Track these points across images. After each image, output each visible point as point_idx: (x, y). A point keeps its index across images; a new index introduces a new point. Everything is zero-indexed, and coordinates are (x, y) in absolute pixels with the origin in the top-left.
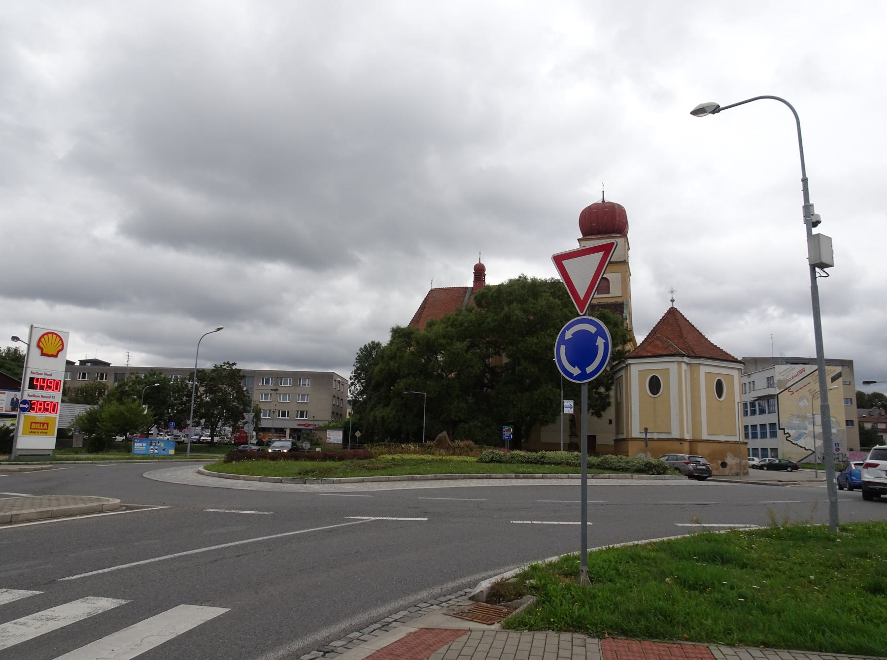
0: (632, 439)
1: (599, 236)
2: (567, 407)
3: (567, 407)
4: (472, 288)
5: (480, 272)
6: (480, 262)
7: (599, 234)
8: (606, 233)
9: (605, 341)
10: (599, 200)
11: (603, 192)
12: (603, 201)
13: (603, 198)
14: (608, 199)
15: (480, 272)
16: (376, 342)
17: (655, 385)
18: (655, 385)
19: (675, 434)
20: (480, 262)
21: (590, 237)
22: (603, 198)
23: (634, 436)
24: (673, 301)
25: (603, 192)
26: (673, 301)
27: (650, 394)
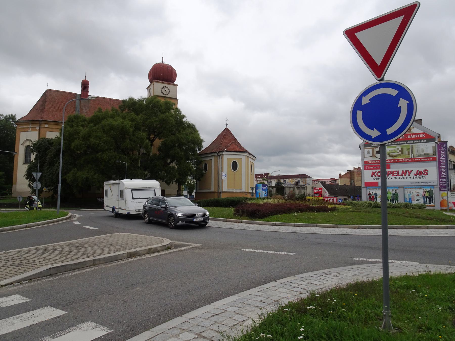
0: (223, 192)
1: (164, 82)
2: (224, 175)
3: (224, 175)
4: (80, 95)
5: (85, 85)
6: (85, 79)
7: (163, 80)
8: (167, 81)
9: (373, 138)
10: (160, 61)
11: (163, 57)
12: (163, 63)
13: (163, 61)
14: (165, 62)
15: (85, 85)
16: (13, 115)
17: (235, 166)
18: (235, 166)
19: (244, 190)
20: (85, 79)
21: (159, 81)
22: (163, 61)
23: (224, 191)
24: (227, 125)
25: (163, 57)
26: (227, 125)
27: (233, 170)
